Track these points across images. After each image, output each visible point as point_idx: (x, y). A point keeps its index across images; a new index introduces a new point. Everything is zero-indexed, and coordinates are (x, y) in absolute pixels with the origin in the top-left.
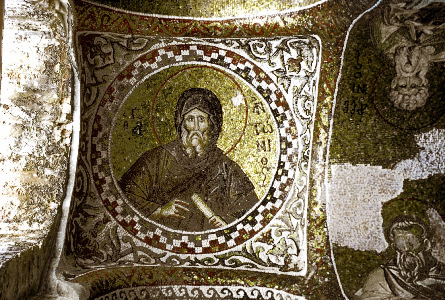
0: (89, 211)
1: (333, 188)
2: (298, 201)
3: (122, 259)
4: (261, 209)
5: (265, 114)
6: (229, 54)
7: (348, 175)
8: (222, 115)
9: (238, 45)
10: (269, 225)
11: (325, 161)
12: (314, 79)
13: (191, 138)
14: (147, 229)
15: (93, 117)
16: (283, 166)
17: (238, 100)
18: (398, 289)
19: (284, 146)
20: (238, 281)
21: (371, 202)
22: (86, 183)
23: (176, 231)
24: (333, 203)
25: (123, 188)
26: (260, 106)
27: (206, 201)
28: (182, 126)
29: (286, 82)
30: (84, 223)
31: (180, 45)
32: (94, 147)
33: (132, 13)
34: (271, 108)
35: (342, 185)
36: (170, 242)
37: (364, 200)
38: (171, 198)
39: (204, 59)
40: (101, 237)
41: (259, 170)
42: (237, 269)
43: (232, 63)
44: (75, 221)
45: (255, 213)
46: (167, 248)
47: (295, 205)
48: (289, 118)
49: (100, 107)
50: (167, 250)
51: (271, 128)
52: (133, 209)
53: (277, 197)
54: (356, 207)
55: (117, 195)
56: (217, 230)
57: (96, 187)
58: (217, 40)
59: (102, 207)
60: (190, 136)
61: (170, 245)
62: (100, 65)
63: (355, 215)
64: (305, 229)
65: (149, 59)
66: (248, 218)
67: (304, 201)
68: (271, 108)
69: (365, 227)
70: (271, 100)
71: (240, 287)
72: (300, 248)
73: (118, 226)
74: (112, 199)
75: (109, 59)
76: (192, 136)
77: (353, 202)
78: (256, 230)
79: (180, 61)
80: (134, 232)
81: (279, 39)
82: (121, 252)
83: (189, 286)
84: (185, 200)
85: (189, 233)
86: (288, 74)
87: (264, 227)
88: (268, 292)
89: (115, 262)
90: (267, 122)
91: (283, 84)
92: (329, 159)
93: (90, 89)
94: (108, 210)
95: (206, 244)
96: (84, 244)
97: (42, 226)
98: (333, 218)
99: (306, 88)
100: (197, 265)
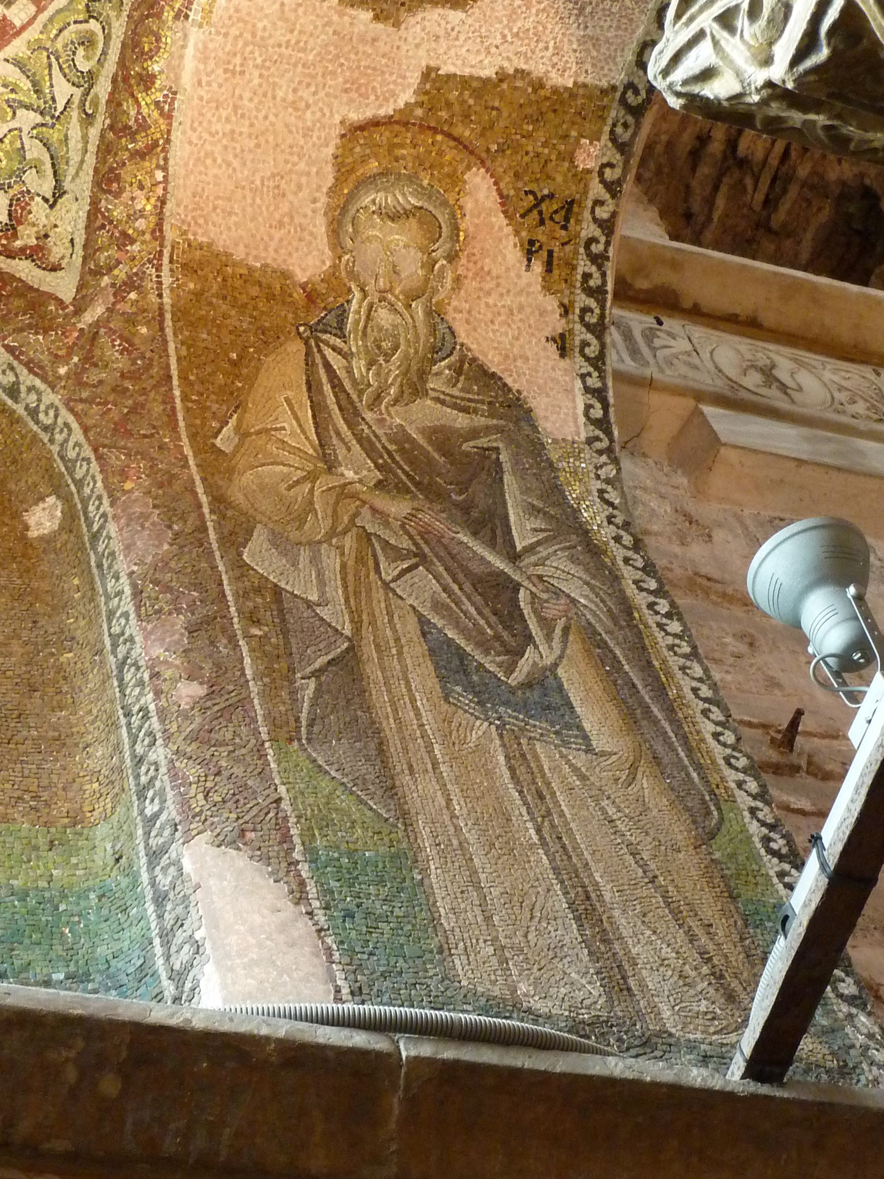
2: (84, 26)
7: (267, 16)
18: (338, 434)
21: (313, 113)
37: (294, 102)
47: (70, 33)
54: (266, 118)
63: (258, 146)
64: (94, 133)
67: (107, 38)
69: (278, 187)
72: (67, 185)
77: (260, 102)
98: (190, 143)
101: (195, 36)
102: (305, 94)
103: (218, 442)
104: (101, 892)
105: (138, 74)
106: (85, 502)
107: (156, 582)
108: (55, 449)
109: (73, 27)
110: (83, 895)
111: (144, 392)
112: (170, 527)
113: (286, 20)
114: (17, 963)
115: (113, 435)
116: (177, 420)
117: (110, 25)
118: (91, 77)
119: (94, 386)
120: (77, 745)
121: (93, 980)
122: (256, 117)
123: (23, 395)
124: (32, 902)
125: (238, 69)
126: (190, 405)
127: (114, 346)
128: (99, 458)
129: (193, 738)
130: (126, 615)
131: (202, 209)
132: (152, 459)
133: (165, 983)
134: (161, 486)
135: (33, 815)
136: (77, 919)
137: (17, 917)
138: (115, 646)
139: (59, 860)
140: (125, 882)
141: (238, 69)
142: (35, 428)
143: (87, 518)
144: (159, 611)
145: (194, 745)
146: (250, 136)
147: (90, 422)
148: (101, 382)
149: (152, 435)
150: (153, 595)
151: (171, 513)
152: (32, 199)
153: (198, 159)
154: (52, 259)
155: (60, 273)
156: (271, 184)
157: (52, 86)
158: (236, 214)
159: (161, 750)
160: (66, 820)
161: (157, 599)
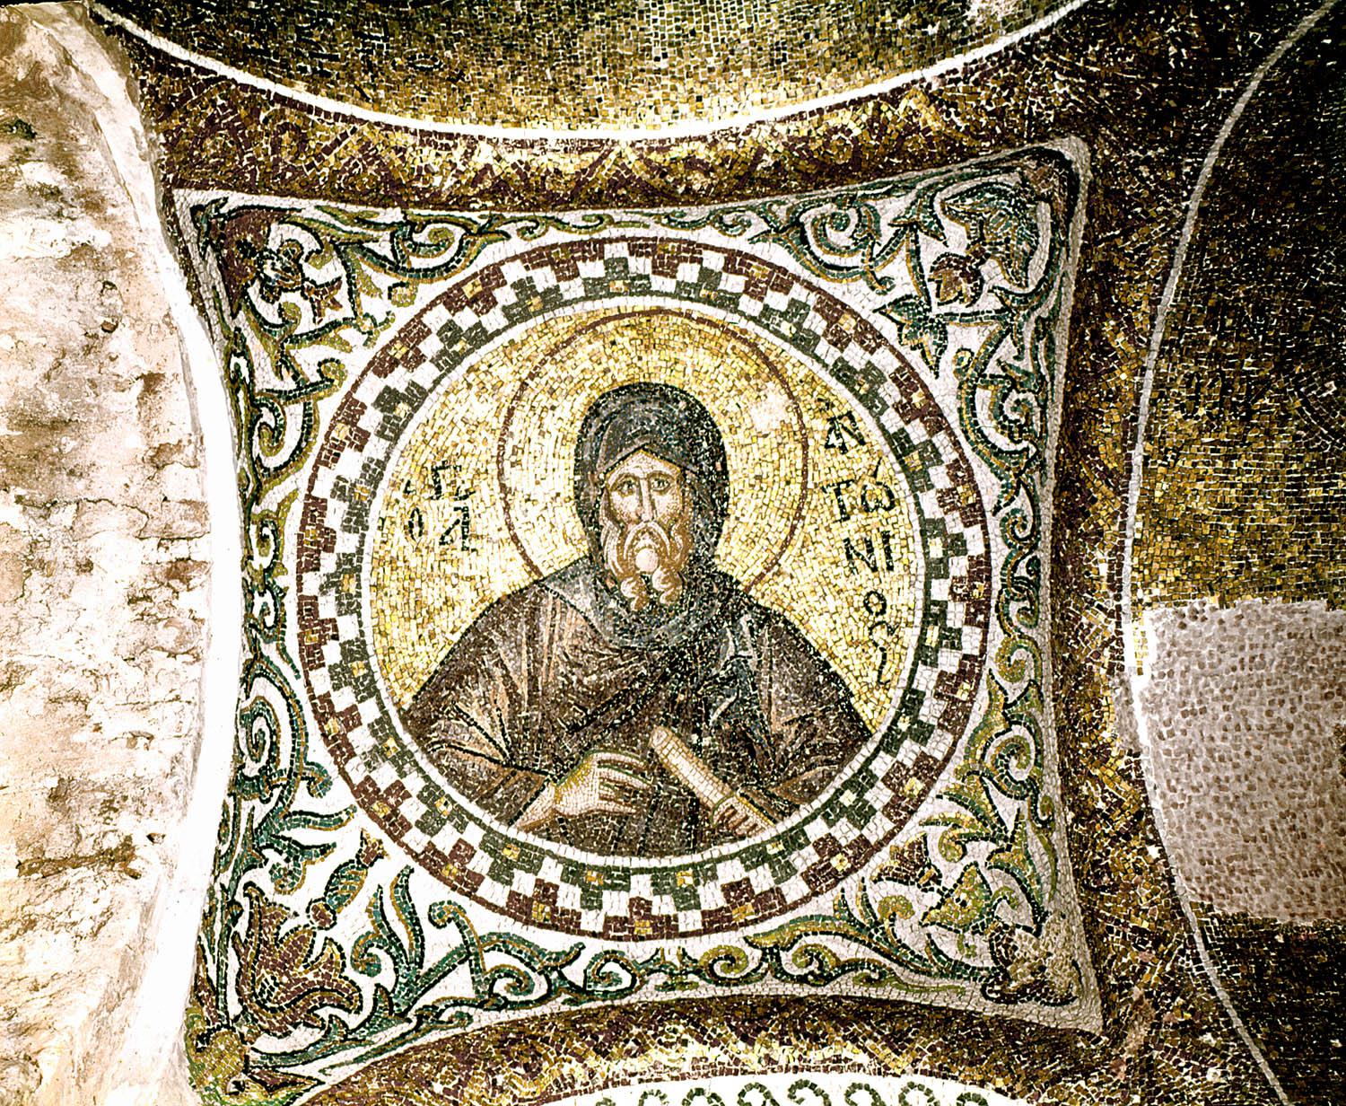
0: (305, 836)
1: (1158, 691)
2: (1009, 735)
3: (428, 999)
4: (881, 766)
5: (865, 448)
6: (735, 262)
7: (1208, 640)
9: (766, 227)
10: (915, 819)
11: (1118, 598)
13: (631, 546)
14: (510, 865)
15: (297, 508)
19: (936, 549)
20: (848, 1051)
21: (1300, 733)
23: (610, 861)
24: (1164, 745)
25: (420, 738)
26: (847, 423)
27: (697, 748)
28: (602, 512)
30: (288, 879)
31: (572, 244)
35: (1190, 679)
36: (591, 899)
37: (1273, 727)
38: (585, 751)
40: (352, 924)
41: (863, 634)
42: (826, 991)
43: (746, 291)
48: (949, 456)
49: (322, 468)
50: (582, 933)
51: (890, 494)
52: (462, 801)
54: (1248, 754)
55: (402, 759)
56: (743, 844)
58: (695, 213)
59: (350, 811)
60: (628, 542)
61: (593, 913)
62: (306, 325)
63: (1251, 788)
65: (475, 300)
66: (842, 799)
69: (1293, 828)
75: (336, 305)
77: (1236, 738)
79: (576, 301)
81: (908, 189)
82: (427, 965)
85: (654, 862)
89: (402, 1016)
90: (875, 475)
91: (920, 346)
93: (272, 410)
94: (373, 816)
95: (711, 897)
98: (1175, 805)
99: (1007, 350)
102: (1282, 713)
113: (1231, 638)
118: (1032, 786)
122: (1238, 756)
125: (1197, 708)
131: (1217, 877)
141: (1197, 708)
152: (1012, 933)
156: (1285, 826)
157: (994, 808)
158: (1260, 872)
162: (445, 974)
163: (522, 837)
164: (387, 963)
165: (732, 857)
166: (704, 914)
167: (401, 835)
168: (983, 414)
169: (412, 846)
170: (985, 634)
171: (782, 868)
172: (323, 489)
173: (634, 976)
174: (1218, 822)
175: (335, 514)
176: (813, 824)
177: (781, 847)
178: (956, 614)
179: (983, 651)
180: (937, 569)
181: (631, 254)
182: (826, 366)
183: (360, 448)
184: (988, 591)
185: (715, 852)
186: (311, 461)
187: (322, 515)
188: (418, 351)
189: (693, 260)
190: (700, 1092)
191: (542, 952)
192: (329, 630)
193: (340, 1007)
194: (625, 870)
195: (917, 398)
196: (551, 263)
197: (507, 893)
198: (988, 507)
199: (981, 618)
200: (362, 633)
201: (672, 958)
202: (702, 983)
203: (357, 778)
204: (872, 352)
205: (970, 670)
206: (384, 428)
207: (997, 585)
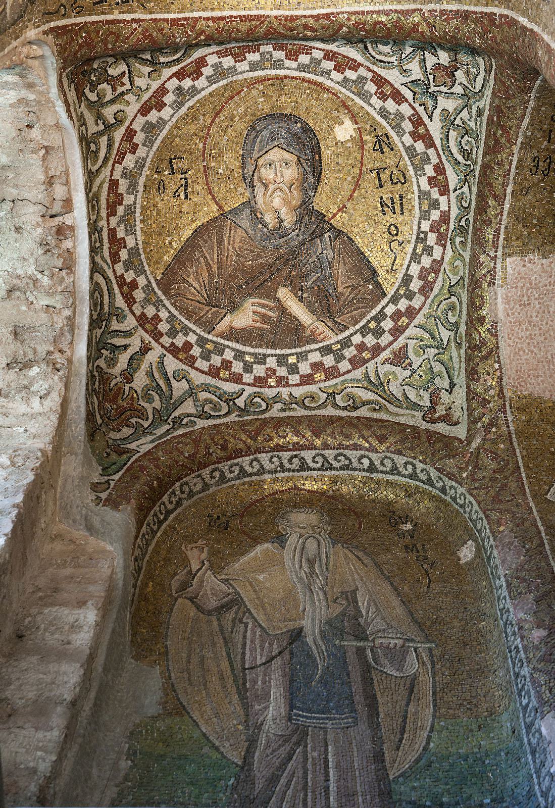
0: (118, 341)
3: (176, 414)
7: (535, 272)
8: (320, 157)
10: (403, 336)
11: (496, 252)
12: (481, 104)
16: (425, 239)
17: (345, 131)
19: (425, 207)
20: (361, 442)
22: (106, 297)
23: (257, 350)
25: (166, 292)
26: (385, 139)
27: (301, 299)
28: (255, 178)
29: (430, 103)
30: (112, 362)
32: (112, 232)
33: (159, 16)
34: (402, 142)
36: (248, 368)
39: (286, 65)
40: (140, 380)
44: (98, 366)
45: (381, 316)
46: (244, 381)
50: (245, 384)
52: (186, 322)
53: (416, 290)
54: (547, 323)
55: (158, 304)
56: (321, 345)
57: (124, 298)
60: (269, 193)
61: (248, 375)
62: (109, 96)
63: (546, 339)
64: (462, 351)
67: (461, 303)
68: (402, 142)
70: (403, 130)
71: (362, 452)
72: (455, 381)
73: (165, 356)
74: (151, 311)
75: (123, 84)
76: (273, 192)
78: (383, 345)
79: (244, 72)
80: (191, 361)
83: (285, 453)
84: (267, 297)
85: (278, 352)
86: (433, 89)
87: (395, 340)
88: (406, 463)
92: (503, 247)
96: (114, 400)
97: (48, 403)
98: (509, 346)
100: (294, 409)
101: (500, 292)
103: (548, 497)
104: (506, 751)
105: (477, 318)
106: (483, 540)
107: (517, 578)
108: (467, 515)
109: (444, 302)
110: (497, 754)
111: (506, 478)
112: (524, 547)
113: (547, 272)
114: (464, 796)
115: (492, 504)
116: (525, 489)
117: (460, 296)
119: (481, 480)
120: (490, 671)
121: (506, 801)
122: (542, 325)
123: (448, 491)
124: (471, 761)
125: (526, 303)
126: (531, 480)
127: (488, 457)
128: (487, 516)
129: (541, 660)
130: (505, 598)
131: (522, 378)
132: (513, 512)
133: (540, 799)
134: (518, 526)
135: (469, 713)
136: (495, 767)
137: (463, 770)
138: (502, 615)
139: (484, 735)
140: (517, 744)
141: (526, 303)
142: (457, 507)
143: (484, 549)
144: (520, 593)
145: (542, 664)
146: (540, 335)
147: (480, 499)
148: (484, 477)
149: (512, 499)
150: (517, 585)
151: (524, 539)
152: (440, 391)
153: (516, 353)
154: (454, 419)
155: (459, 426)
157: (439, 333)
158: (541, 376)
159: (526, 669)
160: (486, 713)
161: (519, 586)
162: (182, 402)
163: (215, 339)
164: (157, 398)
165: (316, 350)
166: (301, 376)
167: (159, 339)
168: (452, 143)
169: (164, 343)
170: (445, 249)
171: (339, 356)
172: (117, 175)
173: (267, 404)
174: (528, 354)
175: (123, 185)
176: (355, 336)
177: (339, 347)
178: (432, 238)
179: (443, 259)
180: (425, 215)
181: (274, 50)
182: (375, 109)
183: (134, 153)
184: (447, 230)
185: (308, 347)
186: (111, 163)
187: (117, 187)
188: (162, 102)
189: (307, 53)
190: (296, 456)
191: (225, 392)
192: (122, 243)
193: (139, 418)
194: (264, 355)
195: (421, 130)
196: (232, 54)
197: (208, 365)
198: (452, 187)
199: (443, 242)
200: (137, 244)
201: (285, 396)
202: (298, 408)
203: (138, 313)
204: (399, 105)
205: (437, 266)
206: (145, 141)
207: (452, 227)
